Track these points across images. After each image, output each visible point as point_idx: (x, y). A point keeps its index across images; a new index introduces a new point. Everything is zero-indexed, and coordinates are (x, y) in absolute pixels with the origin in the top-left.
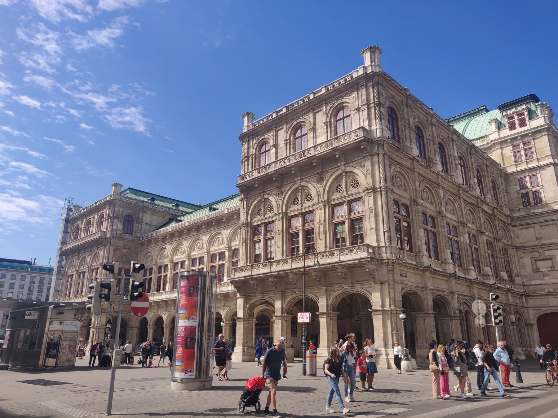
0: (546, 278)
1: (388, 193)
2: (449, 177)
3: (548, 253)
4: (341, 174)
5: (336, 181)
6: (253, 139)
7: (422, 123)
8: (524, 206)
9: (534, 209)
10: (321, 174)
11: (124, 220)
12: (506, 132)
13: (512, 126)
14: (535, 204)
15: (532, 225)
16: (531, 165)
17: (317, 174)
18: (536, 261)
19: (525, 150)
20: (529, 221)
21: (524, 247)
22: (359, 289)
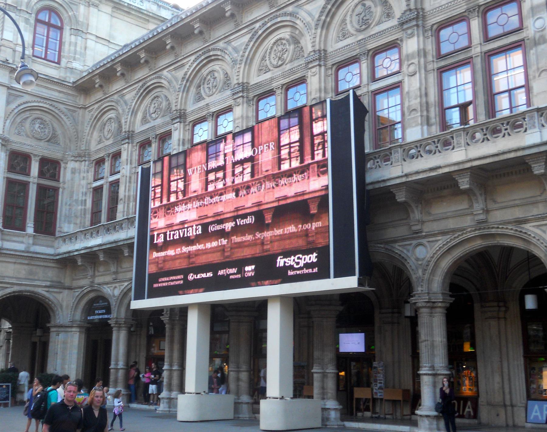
11: (38, 21)
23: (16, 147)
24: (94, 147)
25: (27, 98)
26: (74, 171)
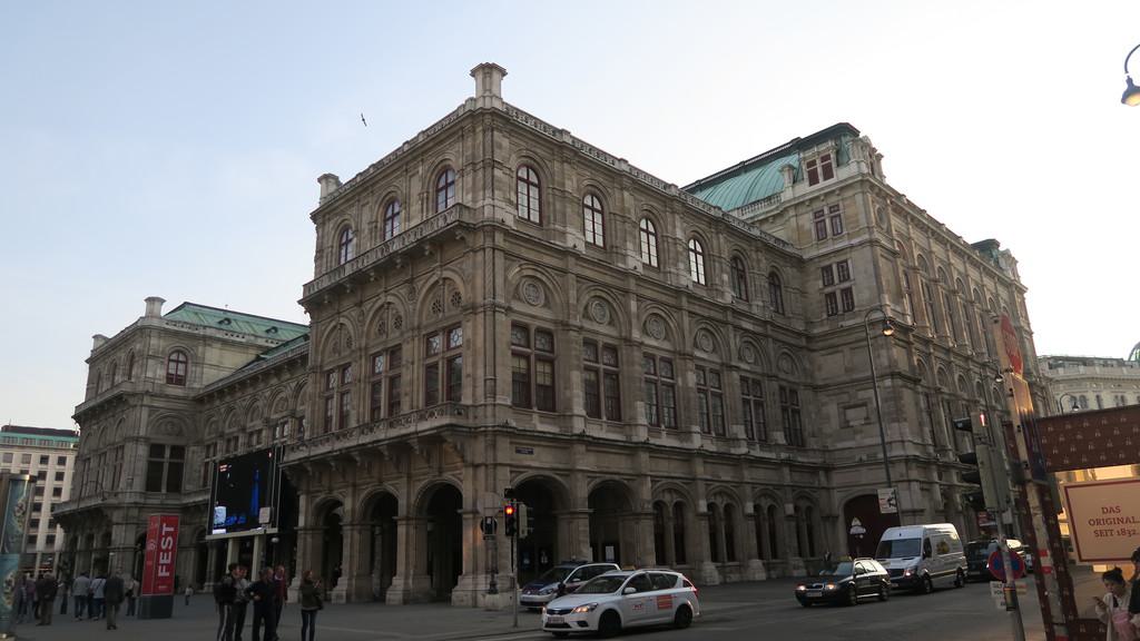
0: (858, 437)
1: (497, 314)
2: (662, 275)
3: (862, 395)
4: (437, 282)
5: (431, 295)
6: (329, 219)
7: (601, 187)
8: (829, 315)
9: (843, 320)
10: (411, 281)
11: (170, 360)
12: (804, 188)
13: (813, 180)
14: (845, 311)
15: (840, 348)
16: (839, 246)
17: (406, 282)
18: (846, 408)
19: (832, 218)
20: (836, 341)
21: (827, 386)
22: (448, 476)
23: (153, 441)
24: (207, 437)
25: (162, 411)
26: (193, 452)
